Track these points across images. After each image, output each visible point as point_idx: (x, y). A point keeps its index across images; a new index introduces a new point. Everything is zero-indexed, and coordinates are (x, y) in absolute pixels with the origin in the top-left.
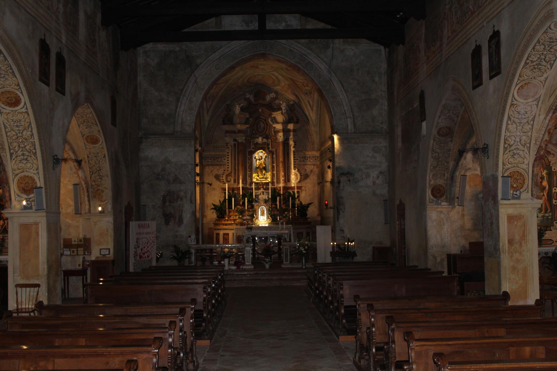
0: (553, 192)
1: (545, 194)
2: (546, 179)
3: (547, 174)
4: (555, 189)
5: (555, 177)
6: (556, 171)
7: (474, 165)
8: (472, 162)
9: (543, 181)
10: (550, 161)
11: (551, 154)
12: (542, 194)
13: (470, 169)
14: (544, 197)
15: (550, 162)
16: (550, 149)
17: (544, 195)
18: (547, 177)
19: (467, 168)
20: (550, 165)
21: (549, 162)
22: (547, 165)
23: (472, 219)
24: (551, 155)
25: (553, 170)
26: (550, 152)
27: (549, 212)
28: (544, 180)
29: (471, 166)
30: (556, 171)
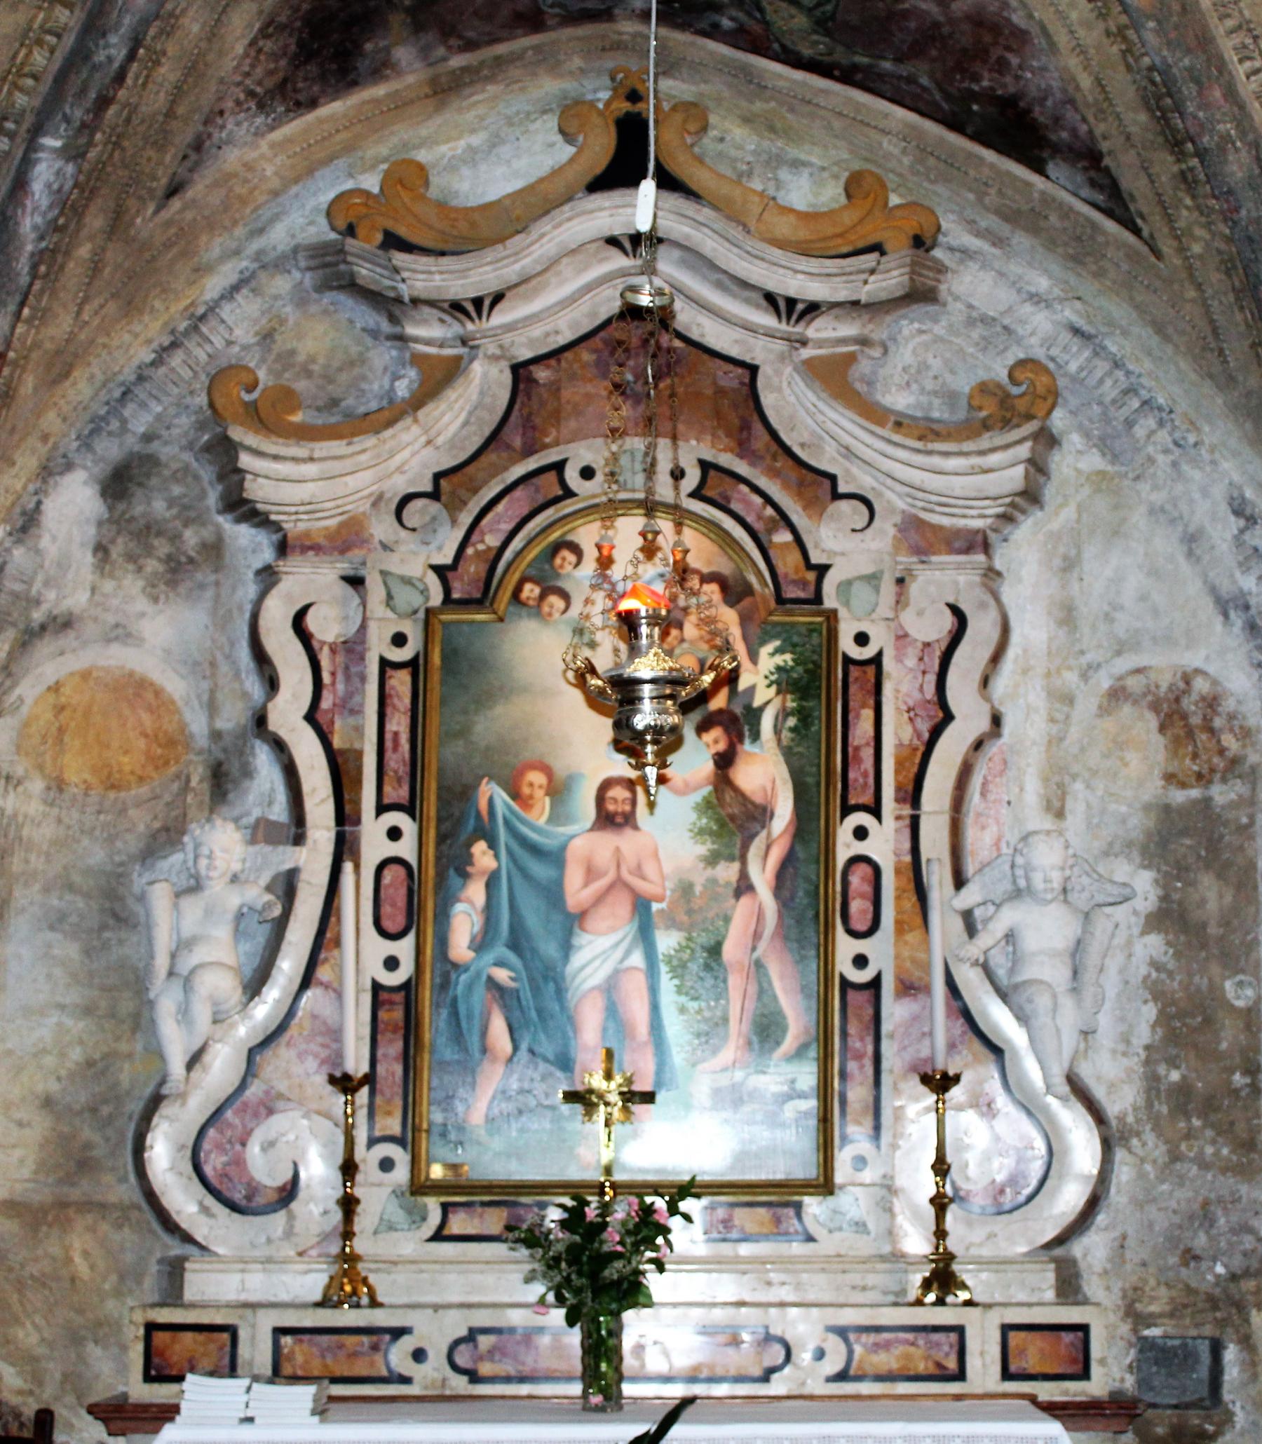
0: (842, 856)
1: (762, 877)
2: (777, 731)
3: (784, 681)
4: (861, 833)
5: (868, 714)
6: (877, 660)
7: (108, 586)
8: (89, 558)
9: (747, 746)
10: (816, 558)
11: (836, 496)
12: (728, 872)
13: (63, 624)
14: (742, 911)
15: (822, 570)
16: (830, 448)
17: (744, 887)
18: (784, 713)
19: (38, 616)
20: (818, 599)
21: (809, 566)
22: (791, 592)
23: (48, 1103)
24: (844, 505)
25: (847, 645)
26: (833, 479)
27: (799, 1053)
28: (756, 736)
29: (78, 600)
30: (877, 660)
